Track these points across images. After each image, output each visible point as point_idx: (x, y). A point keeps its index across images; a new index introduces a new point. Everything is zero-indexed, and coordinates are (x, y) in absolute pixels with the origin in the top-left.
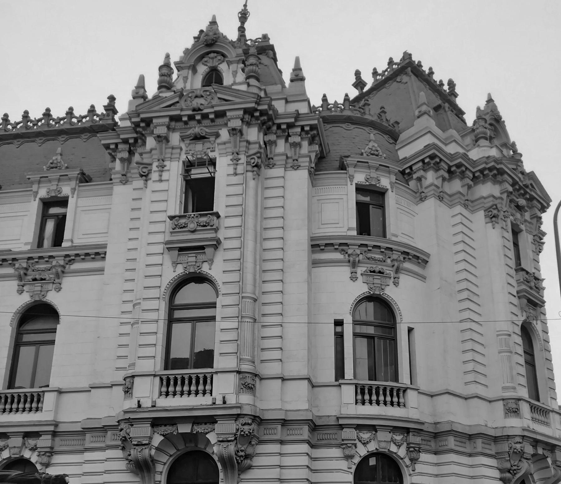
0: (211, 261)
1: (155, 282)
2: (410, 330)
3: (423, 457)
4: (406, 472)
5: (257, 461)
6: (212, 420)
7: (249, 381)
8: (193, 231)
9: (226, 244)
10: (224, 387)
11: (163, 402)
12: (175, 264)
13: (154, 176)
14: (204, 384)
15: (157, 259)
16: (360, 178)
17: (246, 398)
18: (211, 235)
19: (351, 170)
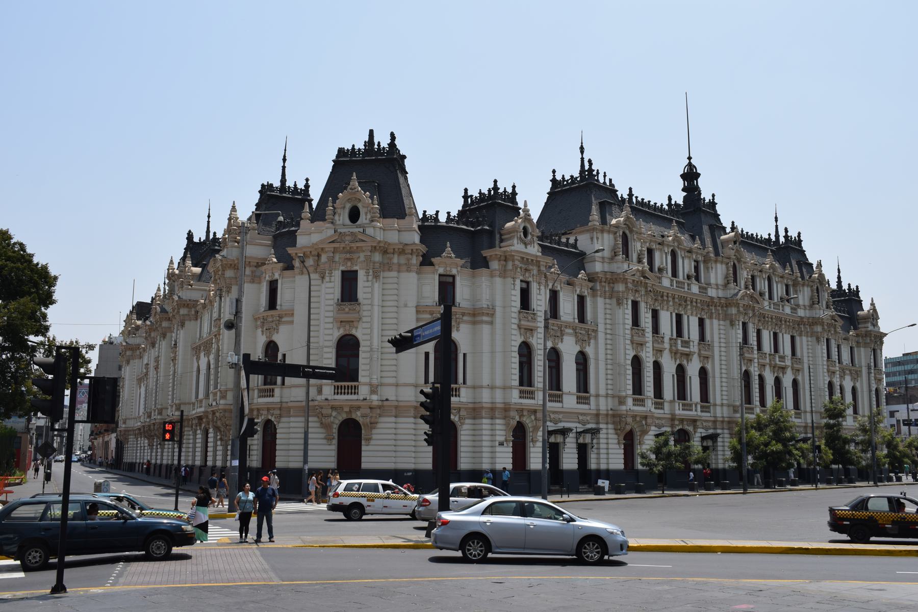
0: (357, 328)
1: (330, 338)
2: (464, 354)
3: (467, 421)
4: (459, 428)
5: (379, 425)
6: (359, 408)
7: (374, 390)
8: (348, 313)
9: (364, 319)
10: (364, 391)
11: (337, 397)
12: (339, 328)
13: (327, 279)
14: (355, 390)
15: (330, 326)
16: (441, 270)
17: (375, 397)
18: (356, 315)
19: (437, 267)
